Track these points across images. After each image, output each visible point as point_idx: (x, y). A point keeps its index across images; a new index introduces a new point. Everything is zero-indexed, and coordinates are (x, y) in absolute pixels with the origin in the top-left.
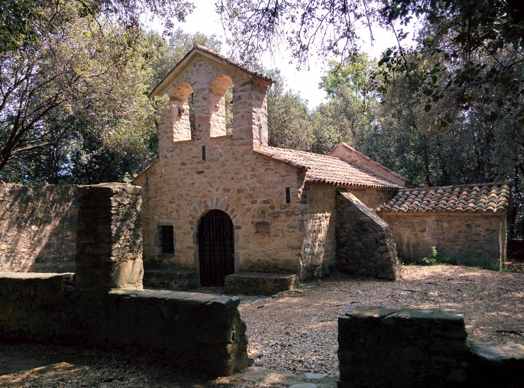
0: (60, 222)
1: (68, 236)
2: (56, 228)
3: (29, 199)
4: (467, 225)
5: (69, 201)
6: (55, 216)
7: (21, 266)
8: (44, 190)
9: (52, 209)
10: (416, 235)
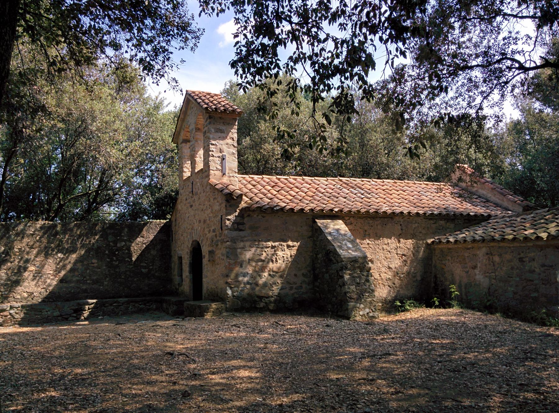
0: (86, 252)
1: (93, 263)
2: (81, 256)
3: (57, 233)
4: (520, 258)
5: (96, 235)
6: (81, 247)
7: (46, 284)
8: (72, 226)
9: (78, 241)
10: (467, 272)
